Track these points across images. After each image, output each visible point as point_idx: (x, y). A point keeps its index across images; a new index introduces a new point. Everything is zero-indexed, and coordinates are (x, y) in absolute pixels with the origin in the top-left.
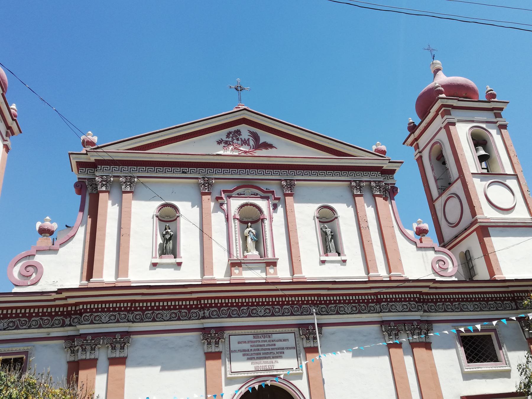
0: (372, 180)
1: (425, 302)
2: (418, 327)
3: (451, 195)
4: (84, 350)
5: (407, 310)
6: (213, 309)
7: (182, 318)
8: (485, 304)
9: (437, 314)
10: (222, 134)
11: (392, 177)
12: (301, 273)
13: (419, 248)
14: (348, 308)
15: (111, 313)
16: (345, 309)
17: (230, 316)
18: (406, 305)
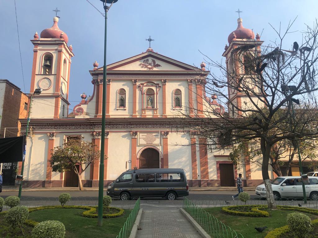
12: (166, 114)
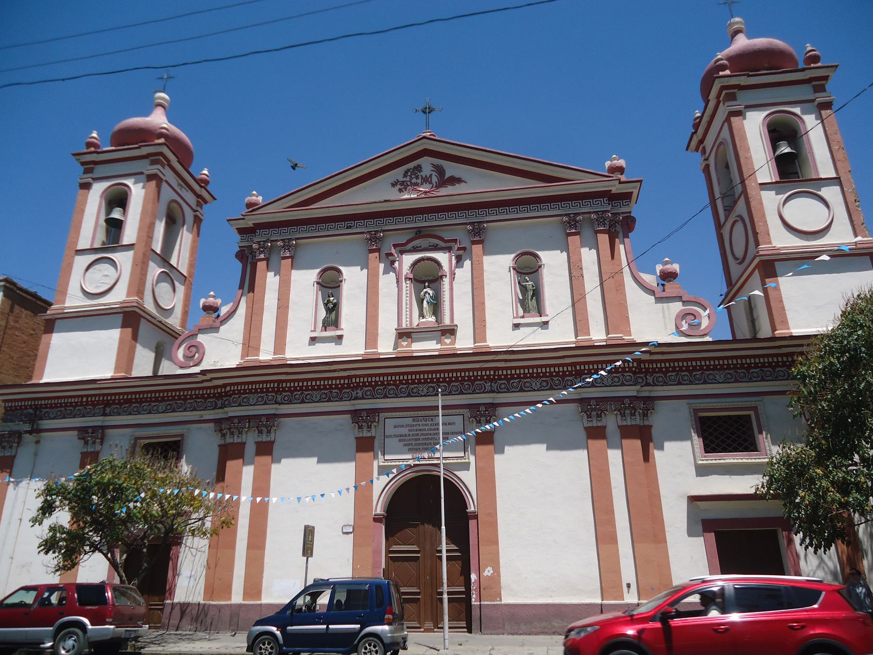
0: (592, 210)
1: (650, 372)
2: (632, 405)
3: (737, 218)
4: (232, 433)
5: (619, 384)
6: (367, 389)
7: (332, 399)
8: (744, 373)
9: (665, 388)
10: (397, 174)
11: (627, 203)
13: (659, 300)
14: (536, 383)
15: (259, 395)
16: (532, 385)
17: (385, 397)
18: (618, 377)
